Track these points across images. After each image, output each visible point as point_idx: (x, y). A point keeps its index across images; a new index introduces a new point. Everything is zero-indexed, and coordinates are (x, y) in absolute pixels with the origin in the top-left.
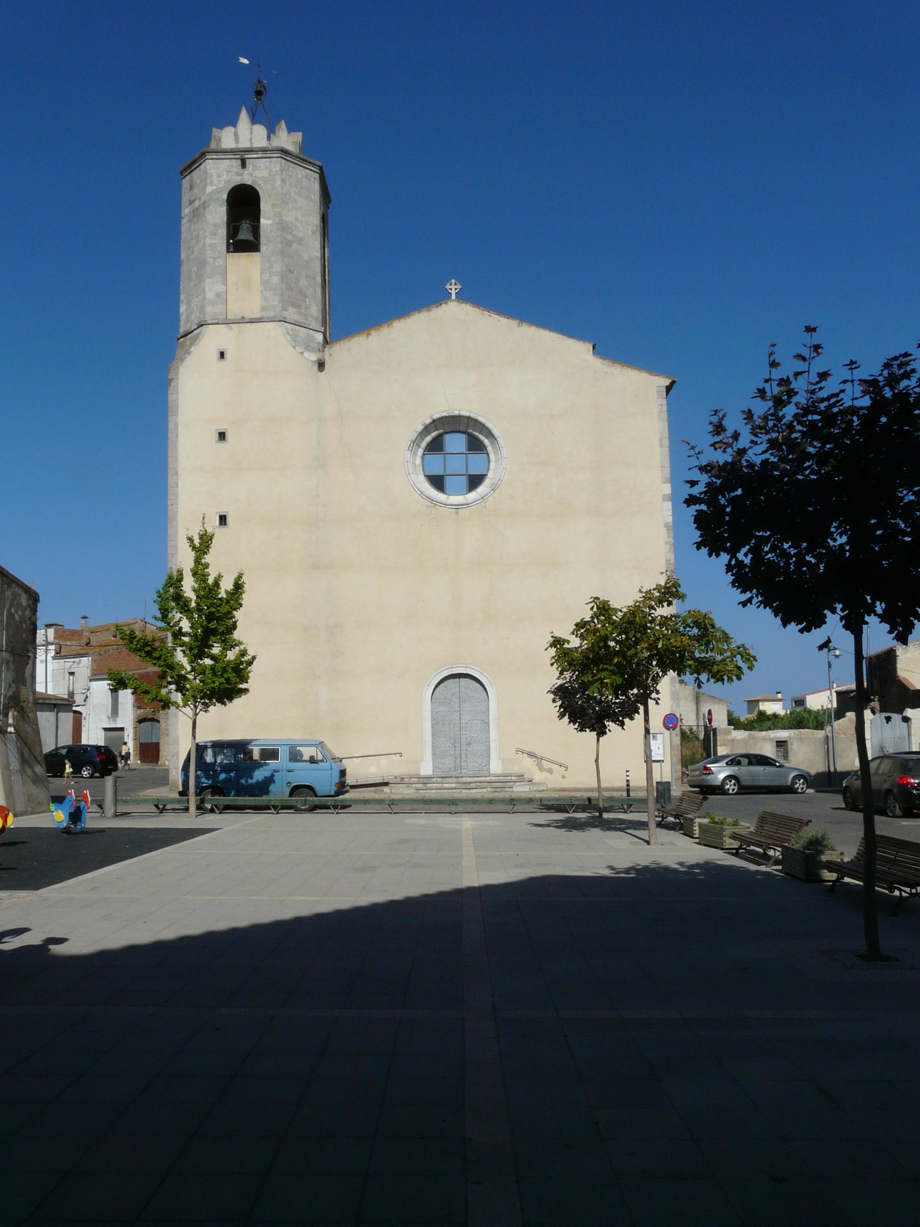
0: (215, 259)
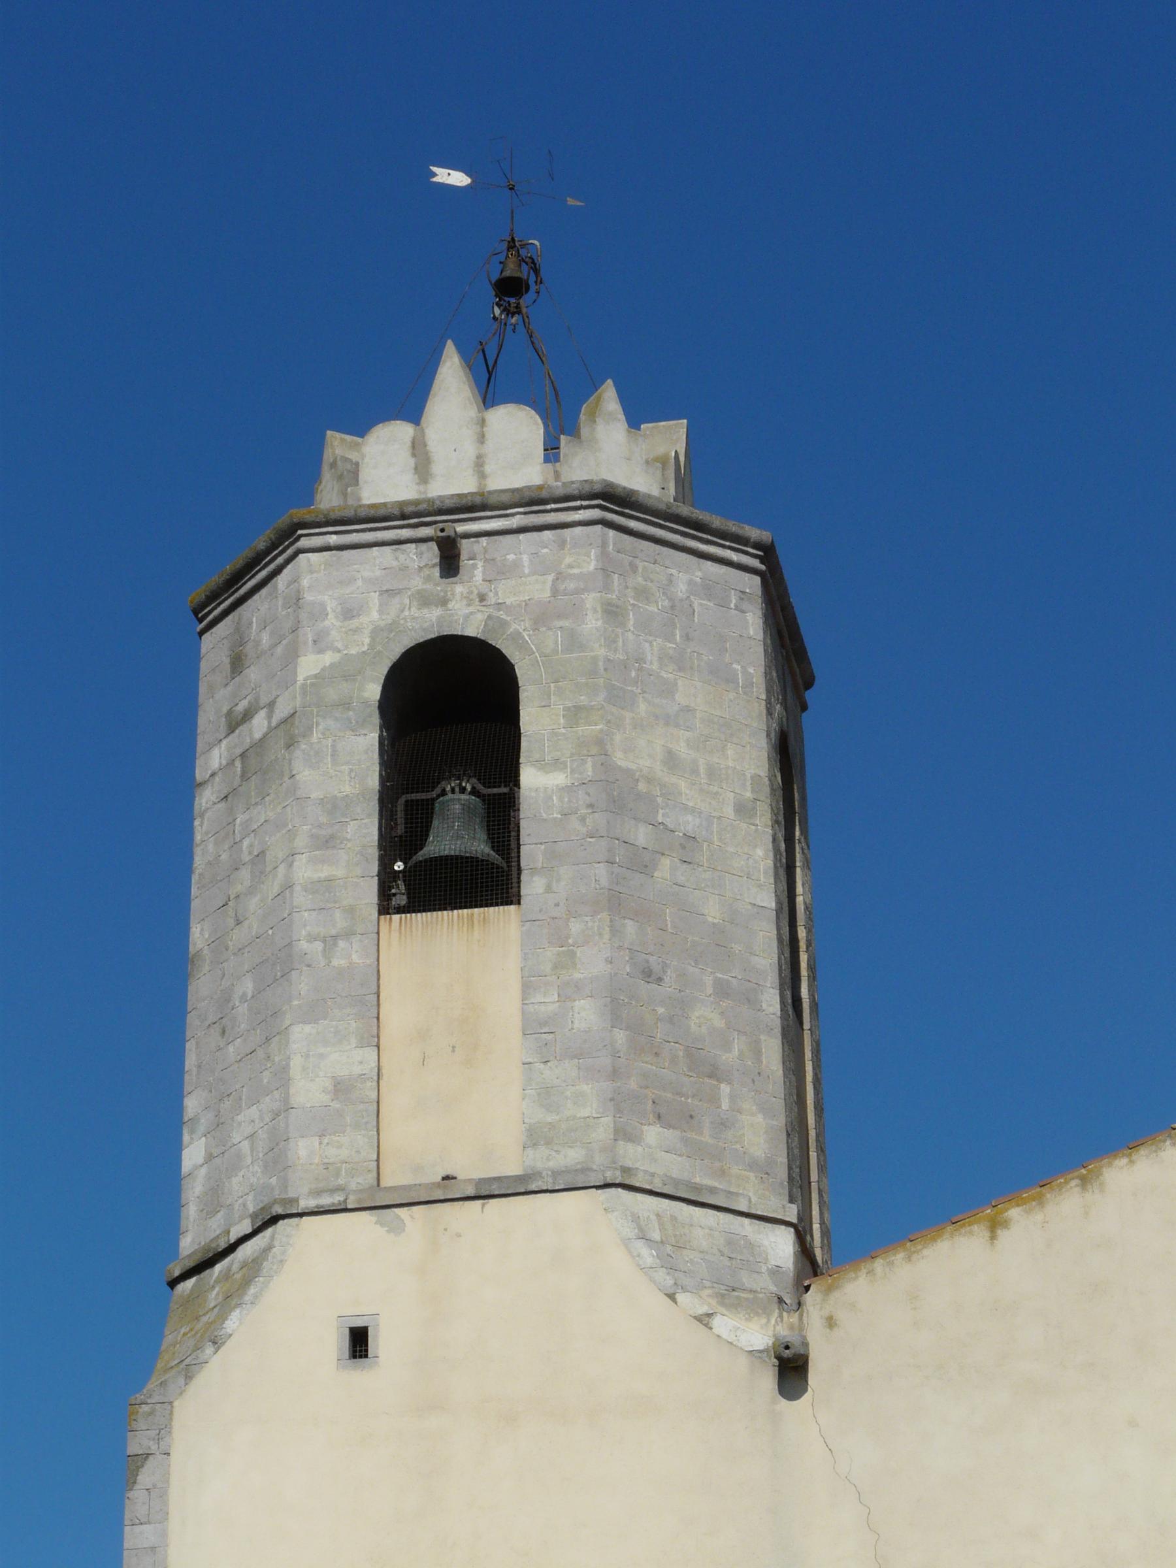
0: (330, 942)
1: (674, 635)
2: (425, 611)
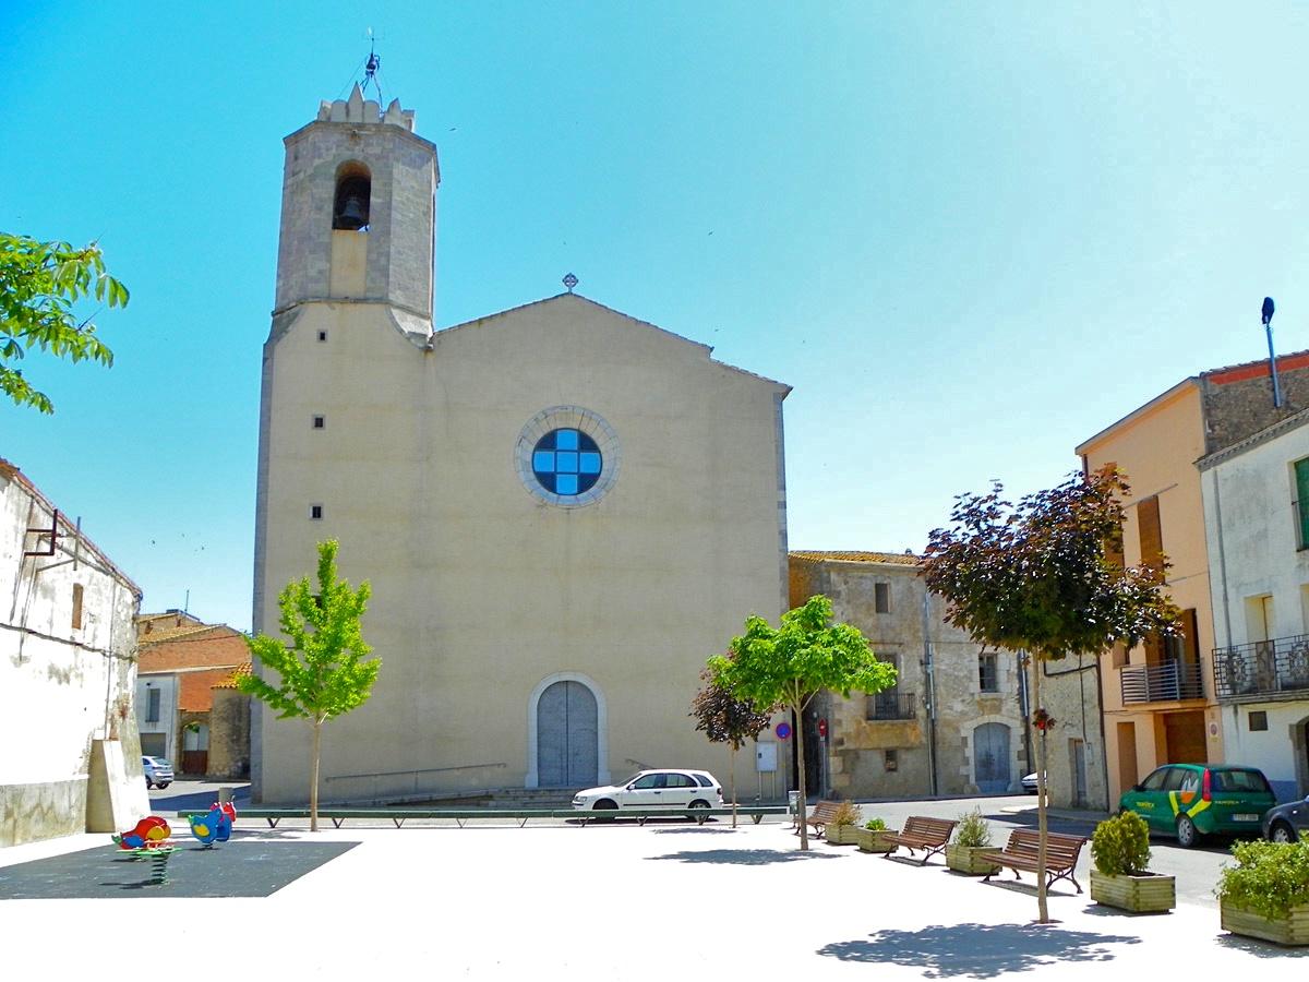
0: (319, 235)
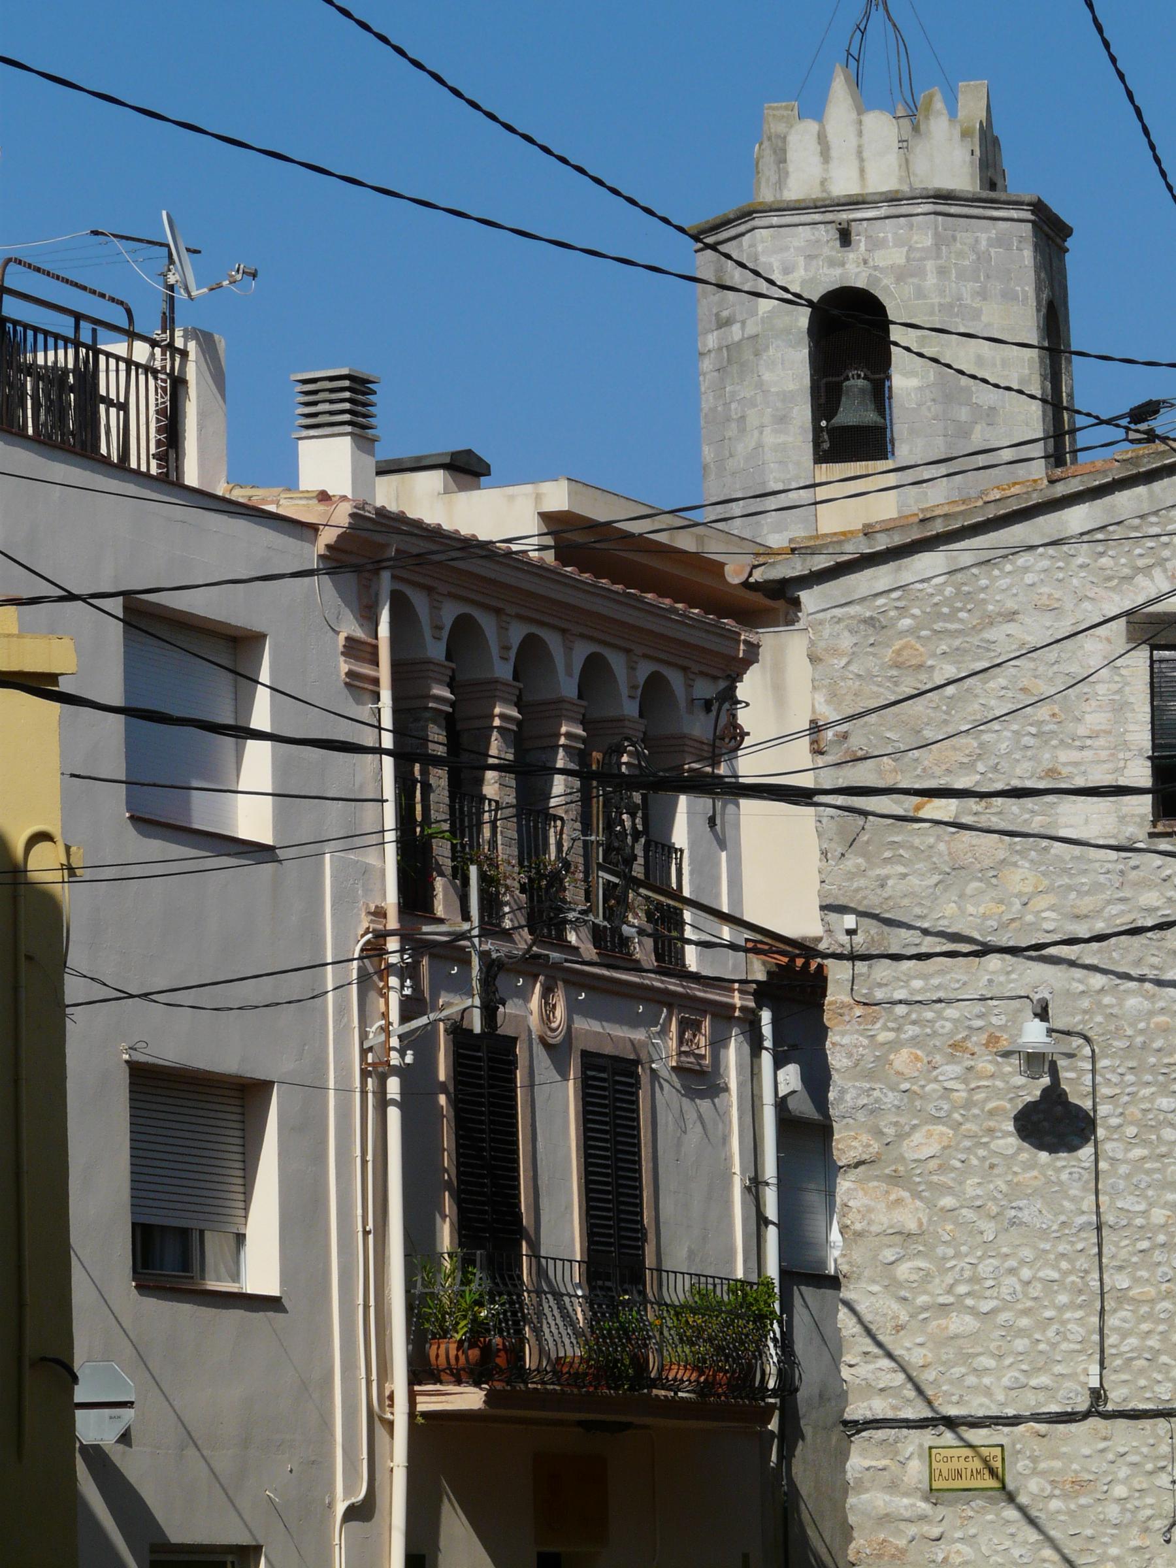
1: (979, 277)
2: (832, 269)
